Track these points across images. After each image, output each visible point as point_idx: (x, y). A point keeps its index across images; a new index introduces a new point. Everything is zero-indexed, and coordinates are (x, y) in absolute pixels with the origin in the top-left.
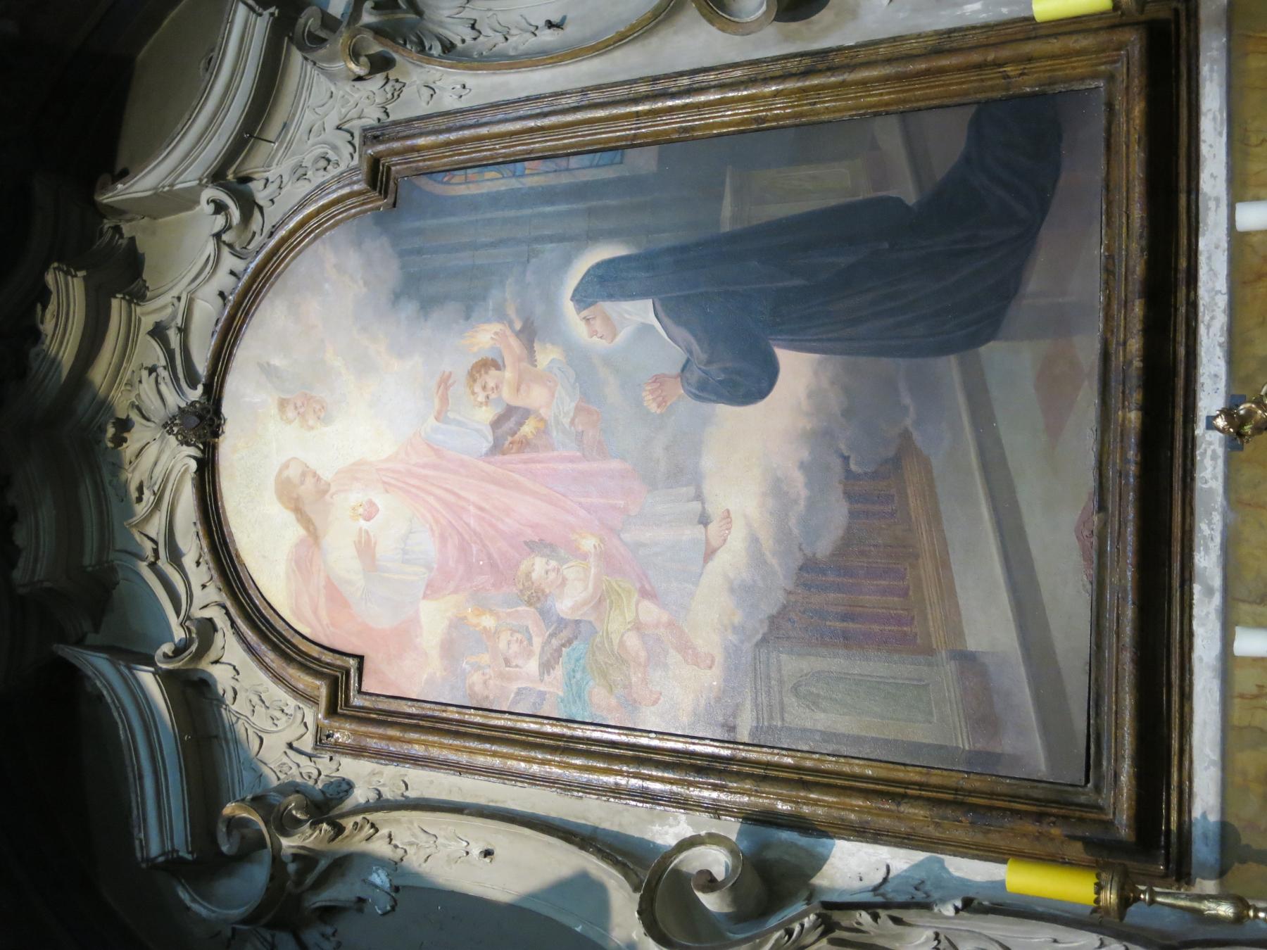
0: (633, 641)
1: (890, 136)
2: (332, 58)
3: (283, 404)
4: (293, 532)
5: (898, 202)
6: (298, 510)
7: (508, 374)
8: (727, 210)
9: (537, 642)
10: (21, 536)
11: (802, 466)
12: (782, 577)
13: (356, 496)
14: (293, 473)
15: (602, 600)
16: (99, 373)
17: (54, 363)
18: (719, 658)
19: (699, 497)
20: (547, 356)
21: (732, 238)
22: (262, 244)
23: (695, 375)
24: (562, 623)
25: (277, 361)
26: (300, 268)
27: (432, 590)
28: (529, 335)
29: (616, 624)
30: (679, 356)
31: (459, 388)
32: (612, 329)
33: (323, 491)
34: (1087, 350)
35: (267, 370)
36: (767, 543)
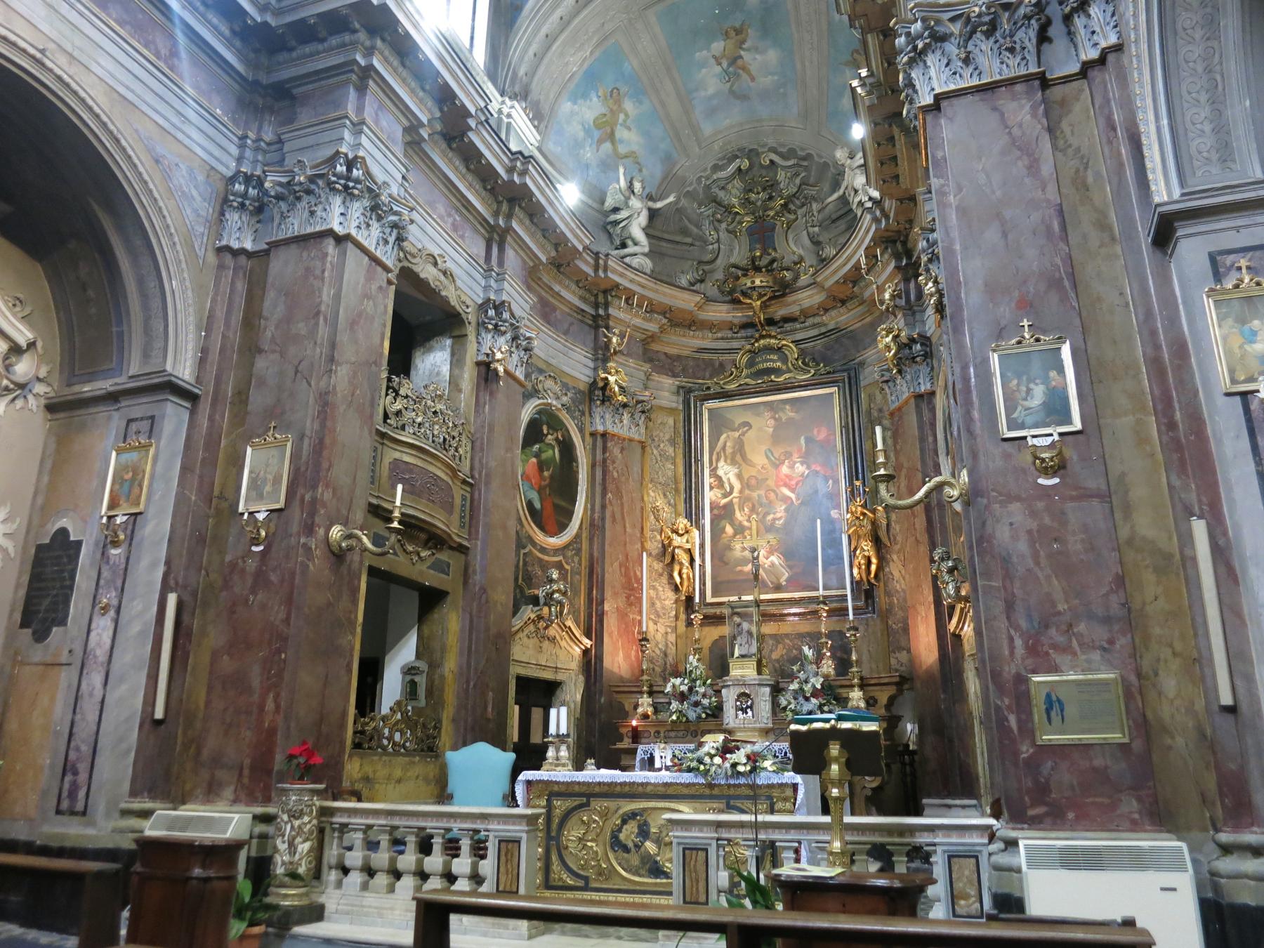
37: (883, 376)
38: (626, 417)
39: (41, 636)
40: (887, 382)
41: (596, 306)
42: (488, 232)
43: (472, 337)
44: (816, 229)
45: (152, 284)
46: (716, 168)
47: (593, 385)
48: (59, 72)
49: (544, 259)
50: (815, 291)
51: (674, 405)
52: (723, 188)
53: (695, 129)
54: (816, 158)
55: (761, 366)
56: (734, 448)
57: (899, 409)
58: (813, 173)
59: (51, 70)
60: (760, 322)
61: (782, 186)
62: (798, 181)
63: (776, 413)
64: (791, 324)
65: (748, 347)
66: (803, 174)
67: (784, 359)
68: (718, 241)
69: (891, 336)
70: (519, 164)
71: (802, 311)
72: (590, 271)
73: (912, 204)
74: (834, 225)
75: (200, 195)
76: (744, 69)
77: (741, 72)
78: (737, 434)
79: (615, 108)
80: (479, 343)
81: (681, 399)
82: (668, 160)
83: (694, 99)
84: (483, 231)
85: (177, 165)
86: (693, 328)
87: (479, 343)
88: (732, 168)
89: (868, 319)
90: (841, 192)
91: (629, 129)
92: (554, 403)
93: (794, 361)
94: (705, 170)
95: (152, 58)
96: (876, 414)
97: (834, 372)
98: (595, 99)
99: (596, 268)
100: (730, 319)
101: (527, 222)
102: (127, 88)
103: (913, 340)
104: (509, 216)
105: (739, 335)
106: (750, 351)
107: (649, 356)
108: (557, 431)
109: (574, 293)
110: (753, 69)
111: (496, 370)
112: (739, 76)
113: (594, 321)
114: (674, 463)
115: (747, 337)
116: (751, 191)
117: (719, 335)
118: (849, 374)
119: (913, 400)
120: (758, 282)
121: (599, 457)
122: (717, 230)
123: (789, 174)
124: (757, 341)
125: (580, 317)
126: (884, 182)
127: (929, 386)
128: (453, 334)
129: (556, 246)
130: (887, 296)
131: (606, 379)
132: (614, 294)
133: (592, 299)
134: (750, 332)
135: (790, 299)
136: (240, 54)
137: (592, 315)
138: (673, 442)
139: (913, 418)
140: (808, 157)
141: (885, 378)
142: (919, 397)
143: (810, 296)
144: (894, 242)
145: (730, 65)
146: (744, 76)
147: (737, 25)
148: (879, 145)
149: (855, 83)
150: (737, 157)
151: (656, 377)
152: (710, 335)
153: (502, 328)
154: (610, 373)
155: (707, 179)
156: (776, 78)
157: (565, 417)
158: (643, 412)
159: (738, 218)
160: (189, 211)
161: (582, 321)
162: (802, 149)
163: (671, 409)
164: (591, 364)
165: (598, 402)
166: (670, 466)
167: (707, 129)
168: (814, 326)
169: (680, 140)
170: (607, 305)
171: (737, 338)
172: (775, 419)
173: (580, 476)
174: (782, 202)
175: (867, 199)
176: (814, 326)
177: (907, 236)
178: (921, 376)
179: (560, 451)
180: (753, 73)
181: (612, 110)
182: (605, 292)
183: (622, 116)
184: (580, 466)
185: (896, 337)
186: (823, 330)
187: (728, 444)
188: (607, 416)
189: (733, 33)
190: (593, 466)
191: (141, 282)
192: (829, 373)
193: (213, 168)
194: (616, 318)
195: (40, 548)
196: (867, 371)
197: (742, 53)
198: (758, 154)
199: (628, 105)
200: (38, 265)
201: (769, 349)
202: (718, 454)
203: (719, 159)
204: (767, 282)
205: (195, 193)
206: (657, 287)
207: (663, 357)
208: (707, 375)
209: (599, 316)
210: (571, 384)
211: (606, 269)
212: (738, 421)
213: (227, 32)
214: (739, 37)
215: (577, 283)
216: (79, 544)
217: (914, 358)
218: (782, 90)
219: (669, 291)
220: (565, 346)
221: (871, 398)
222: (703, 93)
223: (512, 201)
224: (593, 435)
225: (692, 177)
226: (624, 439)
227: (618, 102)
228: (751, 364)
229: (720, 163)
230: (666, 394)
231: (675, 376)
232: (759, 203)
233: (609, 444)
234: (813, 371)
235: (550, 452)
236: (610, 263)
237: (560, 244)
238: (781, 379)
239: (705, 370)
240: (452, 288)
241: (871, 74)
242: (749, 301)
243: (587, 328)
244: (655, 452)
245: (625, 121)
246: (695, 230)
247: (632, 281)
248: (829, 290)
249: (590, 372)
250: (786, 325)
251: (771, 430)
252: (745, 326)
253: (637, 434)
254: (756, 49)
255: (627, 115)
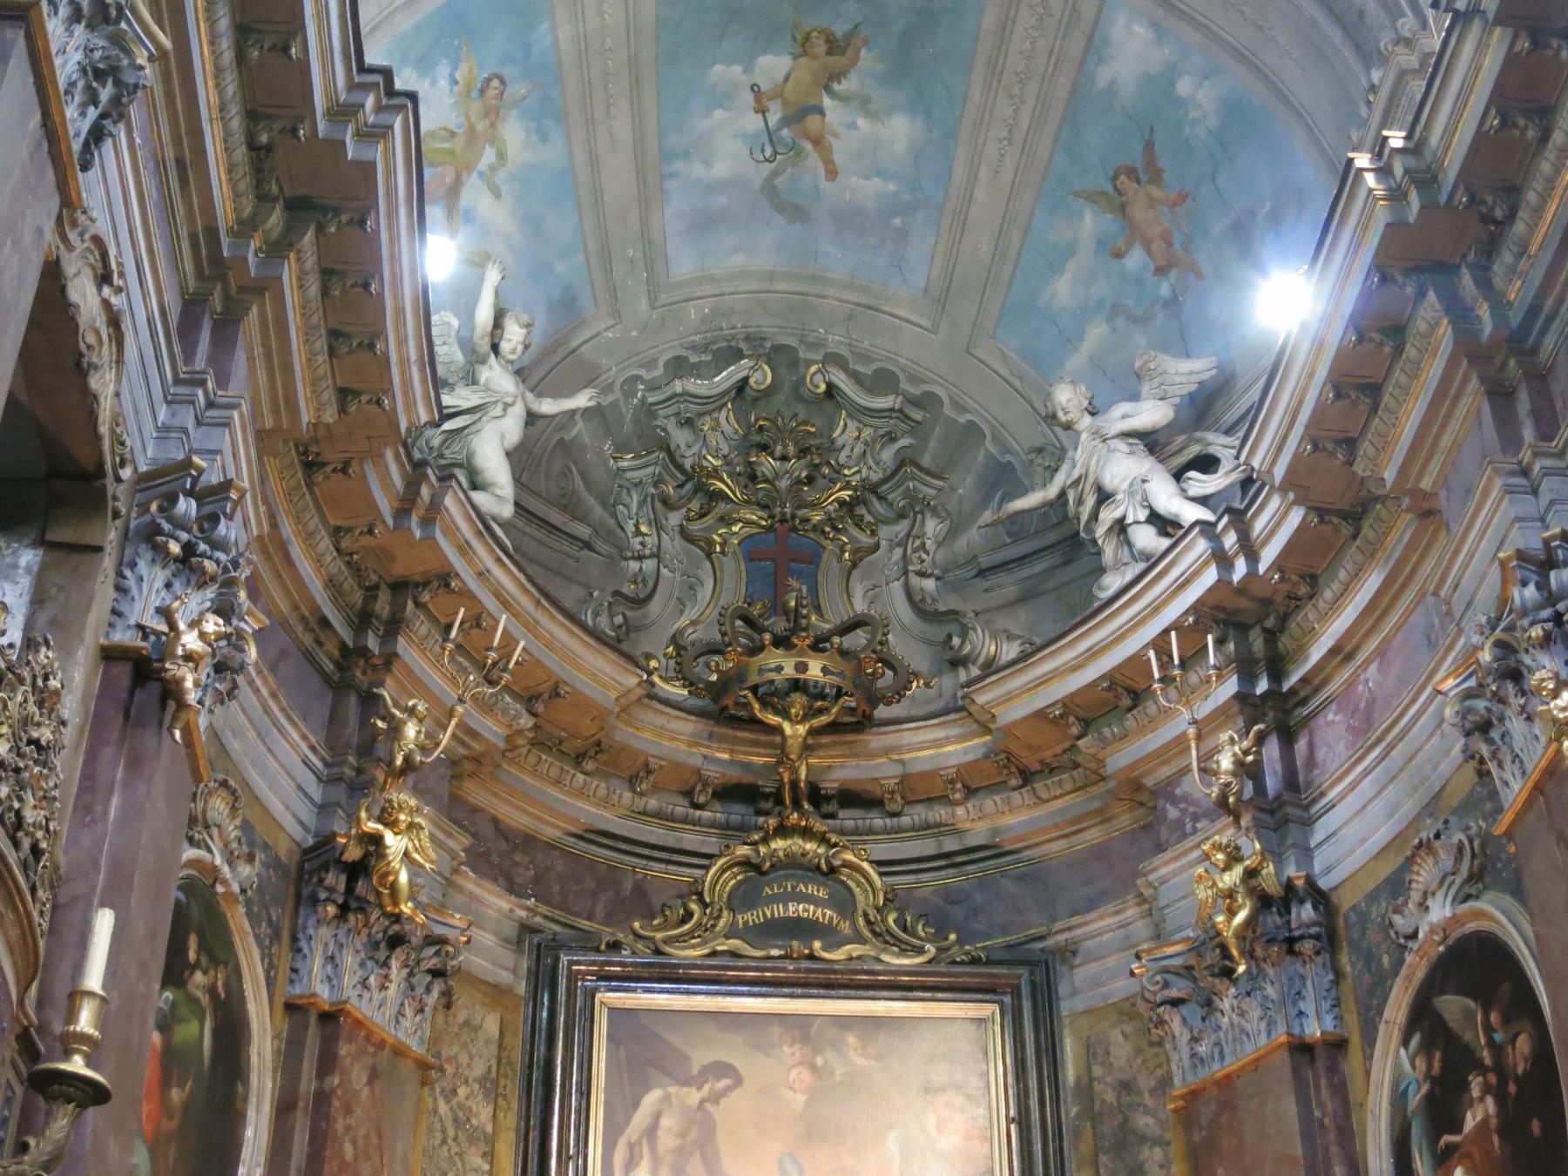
37: (1166, 985)
38: (396, 971)
40: (1175, 1003)
41: (362, 620)
42: (199, 274)
43: (108, 562)
44: (930, 584)
46: (679, 367)
47: (320, 853)
49: (306, 417)
50: (953, 731)
51: (505, 977)
52: (688, 423)
53: (652, 252)
54: (948, 410)
55: (779, 911)
56: (682, 1135)
57: (1226, 1082)
58: (932, 444)
60: (794, 784)
61: (842, 458)
62: (888, 455)
63: (816, 1051)
64: (858, 813)
65: (743, 851)
66: (904, 442)
67: (844, 903)
68: (657, 555)
69: (1238, 870)
70: (370, 102)
71: (904, 780)
72: (385, 506)
73: (1346, 530)
74: (982, 584)
76: (817, 142)
77: (808, 146)
78: (694, 1096)
79: (480, 127)
80: (121, 589)
81: (524, 965)
82: (566, 308)
83: (673, 175)
84: (189, 267)
86: (589, 765)
87: (121, 589)
88: (726, 377)
89: (1093, 836)
90: (1052, 491)
91: (497, 194)
92: (226, 870)
93: (872, 914)
94: (650, 364)
96: (1110, 1096)
97: (989, 963)
98: (443, 83)
99: (402, 513)
100: (697, 762)
101: (314, 289)
103: (1289, 886)
104: (277, 249)
105: (706, 814)
106: (746, 864)
107: (456, 812)
108: (215, 961)
109: (318, 561)
110: (841, 151)
111: (171, 692)
112: (795, 151)
113: (340, 667)
114: (490, 1155)
115: (726, 826)
116: (764, 448)
117: (652, 804)
118: (1032, 973)
119: (1285, 1056)
120: (815, 670)
121: (308, 1084)
122: (659, 528)
123: (867, 433)
124: (765, 840)
125: (308, 639)
126: (1316, 447)
127: (1329, 1023)
128: (51, 536)
129: (344, 395)
130: (1226, 762)
131: (377, 840)
132: (425, 597)
133: (358, 597)
134: (738, 812)
135: (875, 740)
137: (343, 647)
138: (491, 1088)
139: (1290, 1107)
140: (927, 401)
141: (1174, 993)
142: (1301, 1049)
143: (936, 744)
144: (1243, 629)
145: (785, 122)
146: (814, 160)
147: (840, 30)
148: (1361, 338)
149: (1362, 160)
150: (739, 355)
151: (470, 882)
152: (628, 795)
153: (209, 566)
154: (392, 824)
155: (653, 387)
156: (892, 187)
157: (238, 920)
158: (437, 973)
159: (722, 508)
161: (309, 657)
162: (914, 379)
163: (495, 986)
164: (316, 791)
165: (331, 910)
166: (477, 1161)
167: (683, 263)
168: (925, 828)
169: (607, 268)
170: (394, 626)
171: (697, 823)
172: (813, 1068)
173: (249, 1133)
174: (846, 494)
175: (1142, 515)
176: (925, 828)
177: (1284, 619)
178: (1309, 991)
179: (216, 1032)
180: (837, 158)
181: (471, 130)
182: (400, 587)
183: (489, 156)
184: (253, 1100)
185: (1251, 874)
186: (950, 845)
187: (666, 1122)
188: (349, 960)
189: (820, 47)
190: (284, 1109)
192: (975, 961)
194: (409, 672)
196: (1083, 973)
197: (827, 101)
198: (794, 362)
199: (513, 132)
201: (796, 865)
202: (631, 1147)
203: (693, 348)
204: (841, 674)
206: (539, 615)
207: (488, 831)
208: (600, 908)
209: (364, 652)
210: (261, 831)
211: (427, 522)
212: (701, 1057)
214: (831, 60)
215: (337, 532)
217: (1291, 942)
218: (897, 221)
219: (561, 634)
220: (267, 710)
221: (1093, 1051)
222: (698, 170)
223: (298, 207)
224: (291, 1007)
225: (616, 374)
226: (382, 1044)
227: (493, 114)
228: (743, 898)
229: (694, 359)
230: (486, 938)
231: (513, 889)
232: (784, 484)
233: (344, 1050)
234: (931, 949)
235: (194, 1026)
236: (448, 501)
237: (357, 394)
238: (838, 955)
239: (594, 894)
240: (110, 376)
241: (1415, 148)
242: (773, 719)
243: (315, 680)
244: (443, 1108)
245: (493, 169)
246: (598, 512)
247: (483, 575)
248: (1007, 730)
249: (307, 814)
250: (842, 813)
251: (801, 1098)
252: (729, 793)
253: (410, 1033)
254: (863, 104)
255: (501, 156)
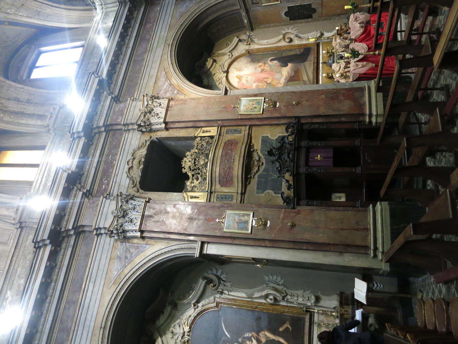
0: (275, 84)
1: (297, 50)
2: (245, 43)
3: (237, 70)
4: (238, 80)
5: (298, 54)
6: (239, 78)
7: (263, 66)
8: (284, 55)
9: (265, 85)
10: (204, 81)
11: (291, 71)
12: (289, 78)
13: (246, 77)
14: (238, 75)
15: (272, 81)
16: (211, 70)
17: (207, 67)
18: (283, 84)
19: (281, 73)
20: (266, 65)
21: (285, 57)
22: (233, 58)
23: (281, 66)
24: (268, 83)
25: (236, 67)
26: (240, 59)
27: (254, 83)
28: (265, 64)
29: (274, 83)
30: (280, 64)
31: (258, 68)
32: (273, 63)
33: (241, 77)
34: (312, 62)
35: (235, 68)
36: (287, 76)
39: (314, 11)
45: (214, 8)
48: (172, 41)
59: (172, 42)
75: (184, 4)
85: (179, 12)
95: (155, 26)
102: (166, 28)
136: (140, 7)
160: (190, 5)
191: (214, 13)
193: (175, 4)
195: (290, 20)
200: (216, 44)
205: (185, 6)
213: (137, 11)
216: (289, 7)
